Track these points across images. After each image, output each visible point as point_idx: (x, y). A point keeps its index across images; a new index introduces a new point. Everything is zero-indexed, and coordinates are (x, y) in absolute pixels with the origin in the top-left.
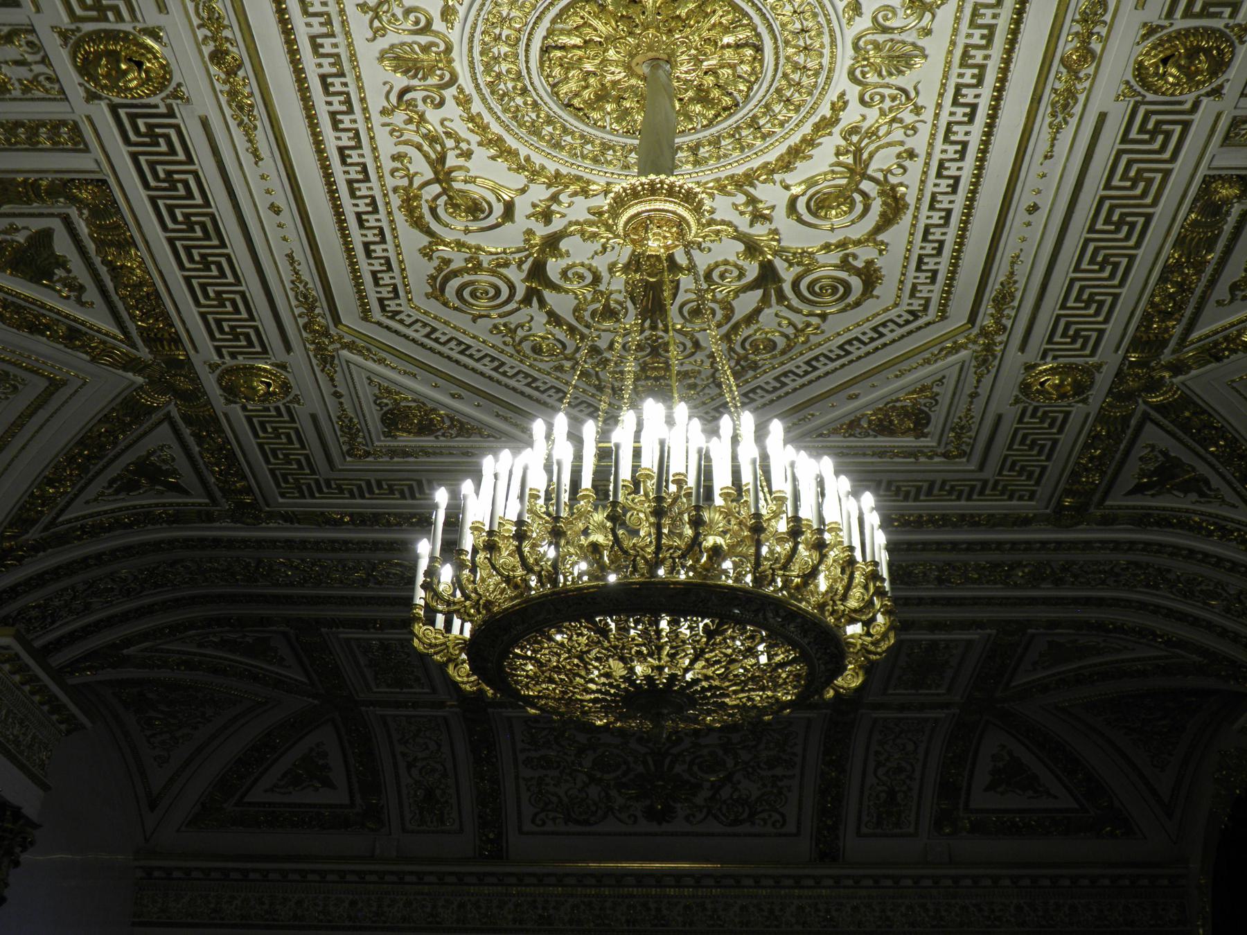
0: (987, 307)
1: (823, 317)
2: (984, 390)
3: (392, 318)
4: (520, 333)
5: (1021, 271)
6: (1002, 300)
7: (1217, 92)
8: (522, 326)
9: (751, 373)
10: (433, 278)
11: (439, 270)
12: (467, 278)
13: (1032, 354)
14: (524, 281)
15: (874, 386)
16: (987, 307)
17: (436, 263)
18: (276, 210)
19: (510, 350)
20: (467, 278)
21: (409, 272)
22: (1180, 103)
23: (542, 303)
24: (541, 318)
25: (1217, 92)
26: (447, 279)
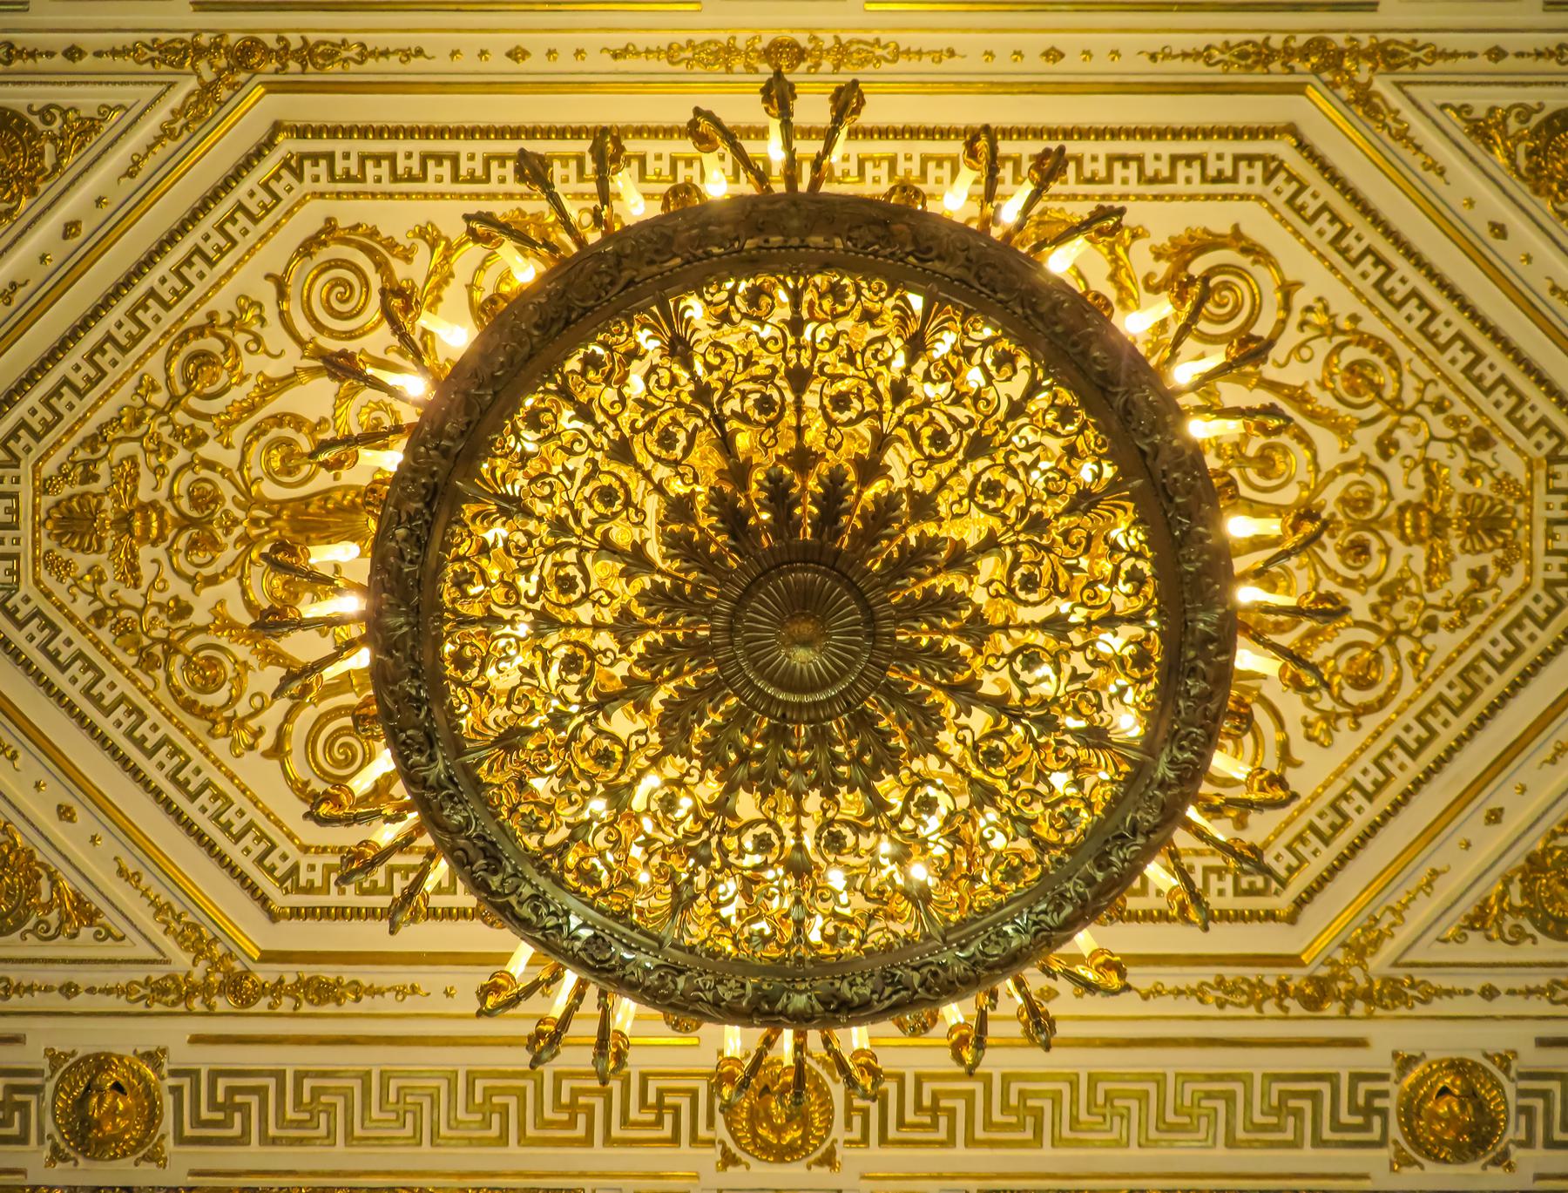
0: (290, 973)
1: (278, 751)
2: (81, 1002)
3: (286, 164)
4: (241, 339)
5: (387, 1004)
6: (324, 992)
7: (729, 1160)
8: (258, 340)
9: (129, 660)
10: (374, 233)
11: (391, 245)
12: (375, 281)
13: (182, 1055)
14: (362, 351)
15: (93, 839)
16: (290, 973)
17: (403, 240)
18: (516, 54)
19: (198, 318)
20: (375, 281)
21: (381, 203)
22: (711, 1123)
23: (314, 372)
24: (275, 369)
25: (729, 1160)
26: (369, 251)
